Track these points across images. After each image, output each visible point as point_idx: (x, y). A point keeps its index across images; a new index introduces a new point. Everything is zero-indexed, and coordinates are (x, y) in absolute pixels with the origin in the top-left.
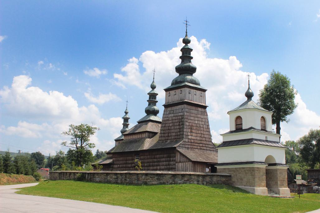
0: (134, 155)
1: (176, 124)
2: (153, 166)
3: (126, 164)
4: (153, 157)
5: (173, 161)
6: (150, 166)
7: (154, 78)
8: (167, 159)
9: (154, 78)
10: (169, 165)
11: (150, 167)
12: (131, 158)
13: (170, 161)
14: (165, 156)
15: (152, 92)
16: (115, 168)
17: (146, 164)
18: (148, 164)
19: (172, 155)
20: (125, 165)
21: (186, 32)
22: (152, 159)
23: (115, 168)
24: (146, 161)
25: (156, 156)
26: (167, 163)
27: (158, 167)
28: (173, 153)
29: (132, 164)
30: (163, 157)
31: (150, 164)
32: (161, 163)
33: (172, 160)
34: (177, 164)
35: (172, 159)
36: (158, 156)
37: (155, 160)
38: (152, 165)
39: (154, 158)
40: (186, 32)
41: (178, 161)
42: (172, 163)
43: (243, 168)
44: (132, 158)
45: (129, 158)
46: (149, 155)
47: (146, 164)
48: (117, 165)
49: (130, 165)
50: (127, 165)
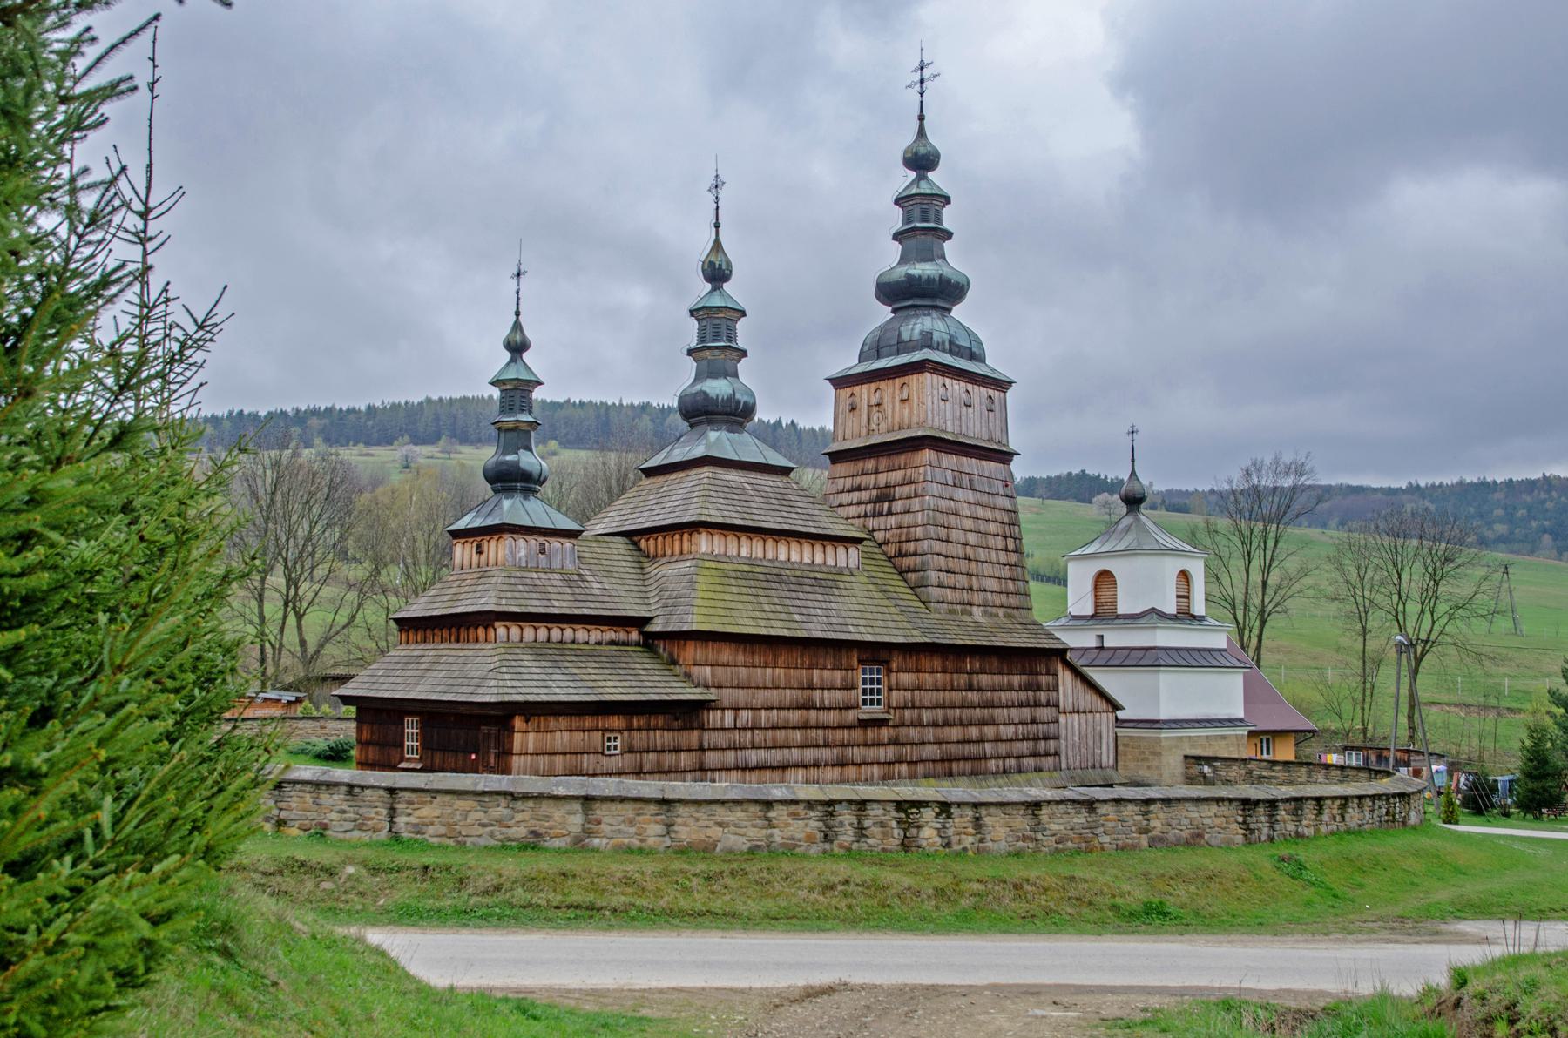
0: (855, 662)
1: (991, 541)
2: (962, 724)
3: (807, 706)
4: (962, 679)
5: (1048, 705)
6: (947, 723)
7: (717, 226)
8: (1023, 695)
9: (717, 226)
10: (1033, 721)
11: (947, 729)
12: (838, 675)
13: (1037, 704)
14: (1016, 680)
15: (717, 301)
16: (723, 729)
17: (927, 716)
18: (940, 712)
19: (1044, 680)
20: (798, 713)
21: (921, 118)
22: (959, 689)
23: (723, 729)
24: (929, 697)
25: (975, 679)
26: (1026, 713)
27: (989, 731)
28: (1048, 673)
29: (848, 708)
30: (1010, 688)
31: (949, 711)
32: (997, 713)
33: (1044, 701)
34: (1062, 719)
35: (1043, 696)
36: (985, 679)
37: (974, 696)
38: (961, 719)
39: (970, 688)
40: (921, 118)
41: (1070, 708)
42: (1044, 713)
43: (1224, 737)
44: (844, 679)
45: (826, 673)
46: (944, 672)
47: (927, 716)
48: (737, 709)
49: (832, 717)
50: (813, 713)
